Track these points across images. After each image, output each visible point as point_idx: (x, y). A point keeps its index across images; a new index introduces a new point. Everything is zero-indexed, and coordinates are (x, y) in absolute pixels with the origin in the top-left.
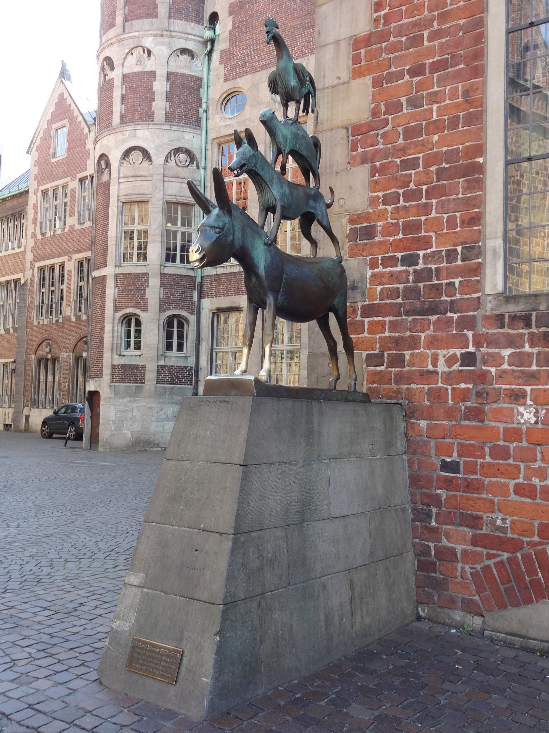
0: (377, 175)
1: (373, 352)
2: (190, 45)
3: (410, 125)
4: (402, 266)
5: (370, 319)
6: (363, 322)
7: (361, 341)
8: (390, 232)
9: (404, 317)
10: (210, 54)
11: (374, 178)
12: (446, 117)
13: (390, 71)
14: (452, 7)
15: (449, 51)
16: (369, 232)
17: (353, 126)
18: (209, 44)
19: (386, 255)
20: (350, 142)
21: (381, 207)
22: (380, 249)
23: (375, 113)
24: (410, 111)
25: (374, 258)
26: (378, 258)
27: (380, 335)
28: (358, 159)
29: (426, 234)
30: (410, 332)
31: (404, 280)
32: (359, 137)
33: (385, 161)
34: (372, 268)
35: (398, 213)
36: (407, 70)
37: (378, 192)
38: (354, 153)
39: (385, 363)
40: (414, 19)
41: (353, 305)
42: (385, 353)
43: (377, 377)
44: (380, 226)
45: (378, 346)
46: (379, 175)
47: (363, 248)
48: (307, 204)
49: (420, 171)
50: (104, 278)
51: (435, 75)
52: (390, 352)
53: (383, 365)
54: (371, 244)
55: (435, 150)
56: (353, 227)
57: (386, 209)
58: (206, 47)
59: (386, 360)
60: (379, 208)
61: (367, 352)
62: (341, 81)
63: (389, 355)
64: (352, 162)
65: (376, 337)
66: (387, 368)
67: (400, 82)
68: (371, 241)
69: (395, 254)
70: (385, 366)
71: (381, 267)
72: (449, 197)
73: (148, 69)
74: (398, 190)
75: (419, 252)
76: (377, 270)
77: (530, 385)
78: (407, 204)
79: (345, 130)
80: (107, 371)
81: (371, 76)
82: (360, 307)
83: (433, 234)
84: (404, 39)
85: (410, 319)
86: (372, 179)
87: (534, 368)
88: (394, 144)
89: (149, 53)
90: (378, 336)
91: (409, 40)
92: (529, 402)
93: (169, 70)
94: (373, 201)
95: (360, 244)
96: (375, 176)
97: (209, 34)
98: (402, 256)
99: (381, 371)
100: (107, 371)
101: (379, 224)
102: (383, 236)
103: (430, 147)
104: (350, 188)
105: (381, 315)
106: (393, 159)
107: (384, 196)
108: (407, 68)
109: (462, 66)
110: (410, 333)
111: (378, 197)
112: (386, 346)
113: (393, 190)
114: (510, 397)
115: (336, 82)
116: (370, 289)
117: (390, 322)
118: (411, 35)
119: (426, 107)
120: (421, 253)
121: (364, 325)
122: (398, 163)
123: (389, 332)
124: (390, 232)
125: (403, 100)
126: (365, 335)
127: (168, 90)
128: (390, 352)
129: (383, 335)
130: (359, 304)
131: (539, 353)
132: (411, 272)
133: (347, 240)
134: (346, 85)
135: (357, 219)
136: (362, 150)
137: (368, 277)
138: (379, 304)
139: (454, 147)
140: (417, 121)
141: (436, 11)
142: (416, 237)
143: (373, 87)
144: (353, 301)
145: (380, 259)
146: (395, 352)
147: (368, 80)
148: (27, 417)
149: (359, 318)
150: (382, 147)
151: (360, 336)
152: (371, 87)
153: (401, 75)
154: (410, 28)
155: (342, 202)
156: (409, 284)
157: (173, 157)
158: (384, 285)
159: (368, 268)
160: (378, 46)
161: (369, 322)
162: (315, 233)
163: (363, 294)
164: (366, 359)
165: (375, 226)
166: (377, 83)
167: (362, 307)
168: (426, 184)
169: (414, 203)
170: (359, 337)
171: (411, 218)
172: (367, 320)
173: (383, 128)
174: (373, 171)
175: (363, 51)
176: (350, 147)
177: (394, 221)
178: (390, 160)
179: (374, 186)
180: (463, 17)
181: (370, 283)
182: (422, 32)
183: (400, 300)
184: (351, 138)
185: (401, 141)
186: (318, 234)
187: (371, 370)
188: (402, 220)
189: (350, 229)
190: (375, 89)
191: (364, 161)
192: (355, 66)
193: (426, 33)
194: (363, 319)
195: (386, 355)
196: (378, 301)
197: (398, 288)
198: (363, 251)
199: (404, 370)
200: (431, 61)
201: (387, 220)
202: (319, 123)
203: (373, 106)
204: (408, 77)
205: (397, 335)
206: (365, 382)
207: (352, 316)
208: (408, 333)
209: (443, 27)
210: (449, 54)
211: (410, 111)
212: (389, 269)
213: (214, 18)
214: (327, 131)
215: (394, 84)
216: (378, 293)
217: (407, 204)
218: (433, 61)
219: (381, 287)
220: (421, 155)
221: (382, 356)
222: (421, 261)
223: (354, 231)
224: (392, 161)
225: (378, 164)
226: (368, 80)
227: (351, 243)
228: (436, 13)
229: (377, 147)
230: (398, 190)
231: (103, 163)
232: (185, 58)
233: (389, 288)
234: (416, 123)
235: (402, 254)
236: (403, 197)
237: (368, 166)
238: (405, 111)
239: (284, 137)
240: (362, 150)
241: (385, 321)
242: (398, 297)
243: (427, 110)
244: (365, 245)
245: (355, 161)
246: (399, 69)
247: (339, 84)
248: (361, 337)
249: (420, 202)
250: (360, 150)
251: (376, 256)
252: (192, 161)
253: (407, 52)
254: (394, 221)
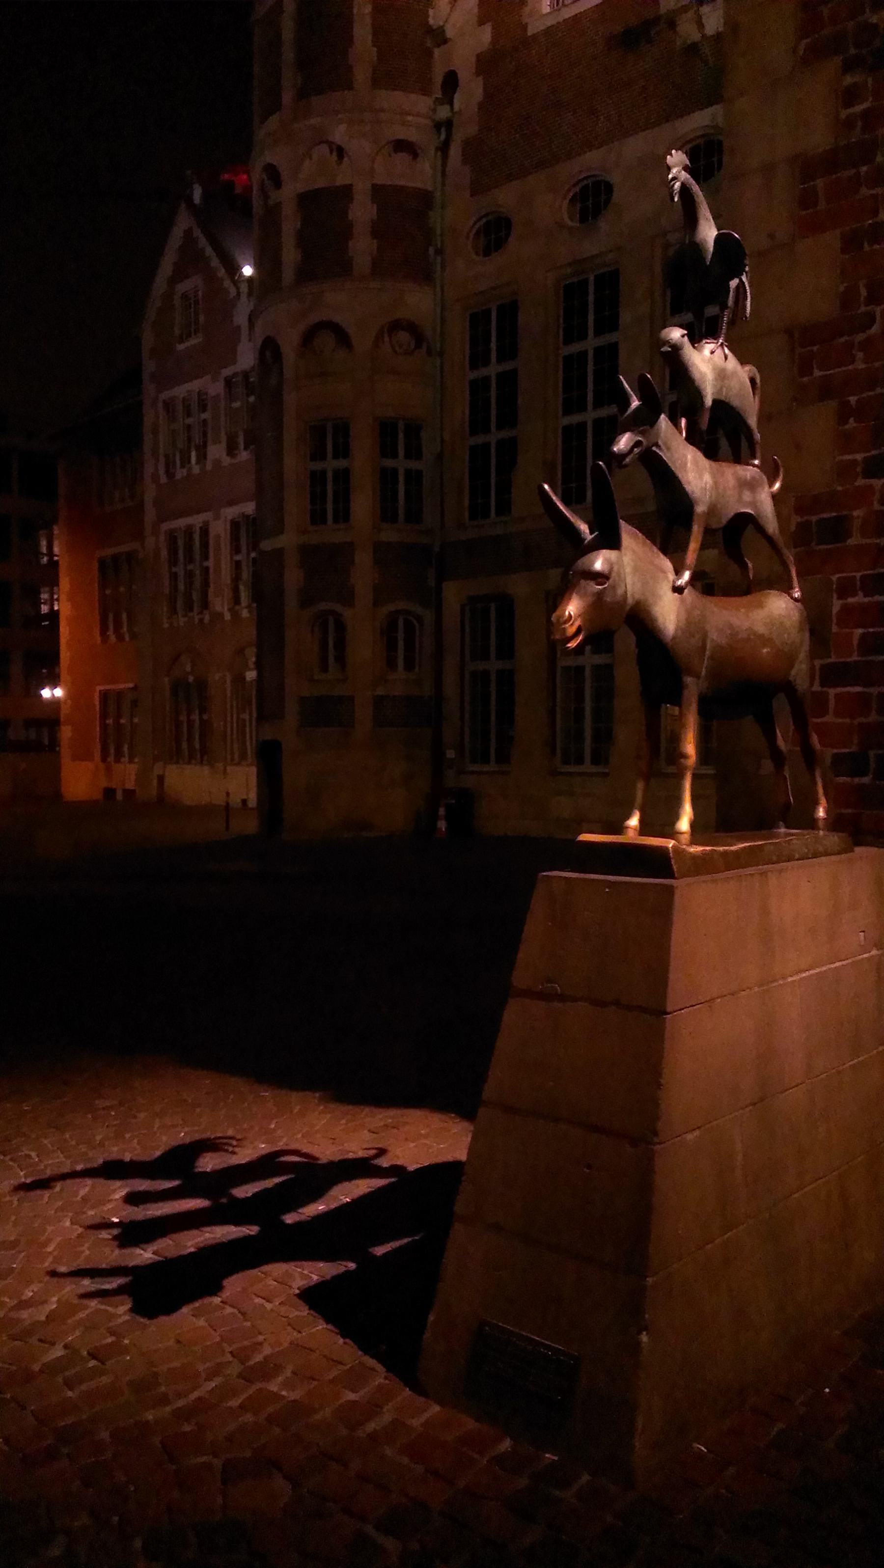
2: (412, 135)
5: (839, 690)
10: (444, 149)
16: (836, 530)
18: (443, 130)
21: (860, 482)
23: (847, 300)
38: (805, 379)
42: (872, 753)
44: (858, 517)
48: (740, 500)
50: (279, 553)
57: (871, 486)
58: (439, 138)
60: (857, 484)
71: (861, 594)
73: (340, 181)
76: (851, 600)
80: (292, 708)
89: (341, 152)
93: (375, 181)
94: (845, 471)
96: (847, 423)
97: (443, 112)
100: (292, 708)
101: (855, 513)
127: (375, 218)
136: (822, 373)
138: (855, 662)
143: (843, 251)
147: (832, 239)
148: (161, 779)
157: (386, 339)
159: (835, 596)
161: (836, 695)
166: (851, 243)
172: (832, 692)
175: (820, 183)
189: (799, 525)
194: (825, 689)
196: (855, 658)
203: (842, 288)
213: (451, 81)
216: (855, 642)
223: (804, 527)
225: (853, 399)
226: (832, 239)
229: (850, 367)
231: (268, 354)
232: (402, 158)
237: (833, 404)
239: (703, 375)
240: (822, 373)
250: (817, 373)
252: (418, 346)
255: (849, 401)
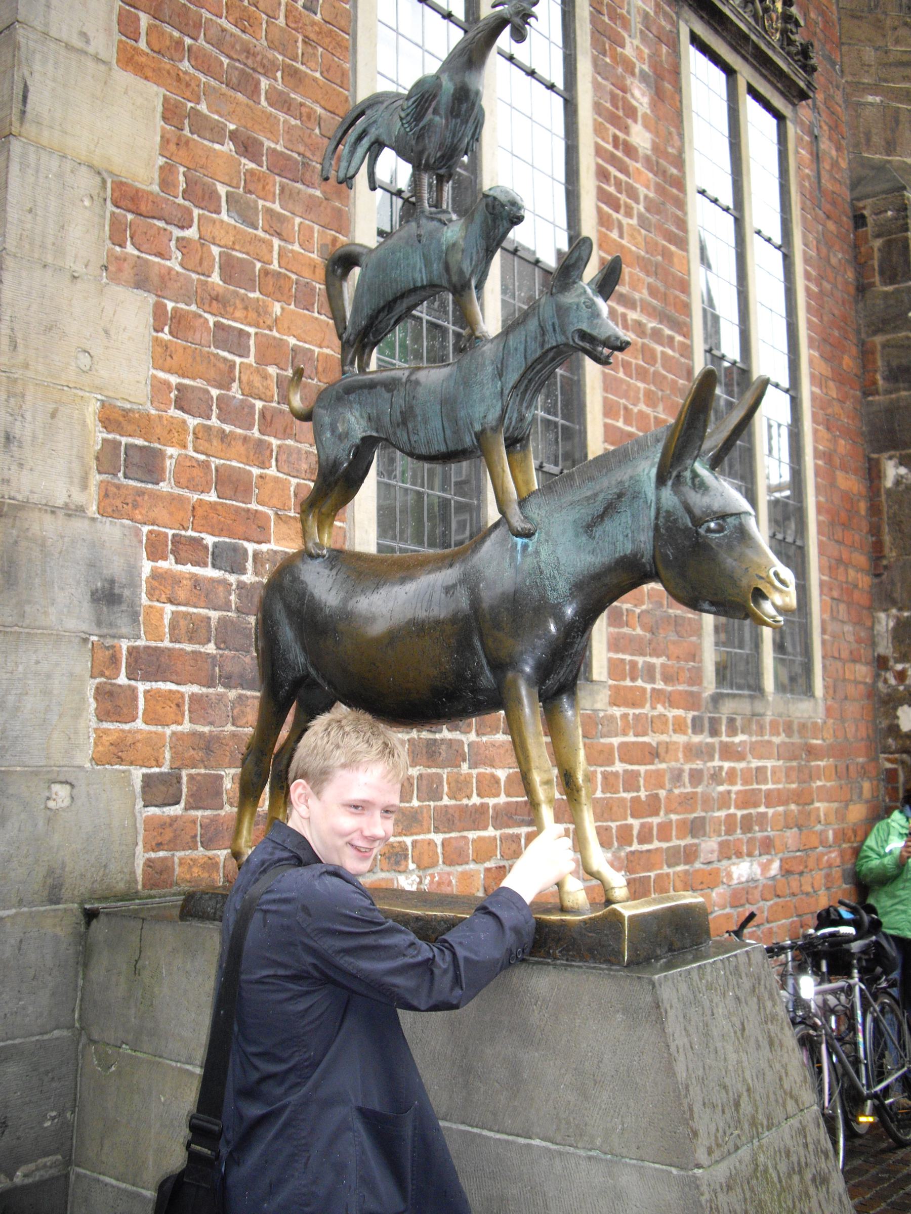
0: (166, 329)
1: (156, 770)
3: (234, 253)
4: (214, 566)
5: (148, 686)
6: (134, 690)
7: (130, 740)
8: (193, 479)
9: (220, 689)
11: (160, 335)
12: (294, 277)
13: (198, 107)
14: (303, 68)
15: (301, 149)
17: (115, 179)
19: (183, 533)
20: (108, 215)
22: (171, 514)
24: (233, 222)
25: (158, 534)
26: (166, 535)
27: (174, 727)
28: (128, 272)
29: (260, 508)
30: (233, 724)
31: (221, 601)
32: (130, 217)
33: (182, 306)
34: (152, 557)
35: (209, 441)
36: (230, 132)
37: (170, 371)
38: (118, 249)
39: (184, 797)
40: (243, 36)
41: (109, 642)
42: (184, 773)
43: (168, 835)
44: (171, 457)
45: (168, 755)
46: (171, 333)
47: (135, 500)
49: (251, 365)
51: (278, 179)
52: (193, 771)
53: (177, 803)
54: (156, 497)
55: (275, 333)
56: (110, 436)
59: (185, 790)
61: (145, 770)
62: (91, 50)
63: (191, 777)
64: (112, 268)
65: (164, 734)
66: (186, 809)
67: (217, 147)
68: (150, 486)
69: (203, 535)
70: (182, 804)
71: (171, 557)
72: (299, 445)
74: (210, 388)
75: (246, 544)
76: (162, 564)
77: (412, 834)
78: (228, 428)
79: (98, 179)
81: (162, 91)
82: (124, 652)
83: (271, 513)
84: (226, 61)
85: (232, 694)
86: (155, 334)
87: (415, 803)
88: (202, 278)
90: (168, 731)
91: (237, 73)
92: (412, 866)
95: (127, 487)
96: (162, 331)
98: (215, 545)
99: (174, 819)
101: (170, 451)
102: (178, 484)
103: (269, 322)
104: (106, 332)
105: (174, 678)
106: (201, 312)
107: (180, 388)
108: (232, 127)
109: (318, 193)
110: (234, 728)
111: (167, 384)
112: (186, 755)
113: (199, 383)
114: (389, 858)
115: (77, 42)
116: (150, 607)
117: (193, 697)
118: (237, 64)
119: (260, 233)
120: (250, 547)
121: (135, 698)
122: (211, 324)
123: (190, 722)
124: (193, 479)
125: (222, 190)
126: (139, 724)
128: (193, 771)
129: (179, 728)
130: (125, 645)
131: (421, 776)
132: (234, 587)
133: (94, 464)
134: (102, 67)
135: (121, 419)
137: (144, 577)
139: (307, 346)
140: (248, 254)
141: (280, 53)
142: (243, 509)
143: (164, 118)
144: (111, 632)
145: (170, 537)
146: (203, 771)
149: (122, 680)
150: (178, 269)
151: (126, 727)
152: (158, 115)
153: (217, 133)
154: (238, 47)
155: (85, 360)
156: (229, 614)
158: (179, 604)
159: (144, 554)
160: (176, 34)
161: (146, 692)
162: (10, 418)
163: (134, 617)
164: (143, 787)
165: (160, 454)
167: (131, 651)
168: (260, 399)
169: (239, 431)
170: (123, 731)
171: (234, 464)
172: (142, 687)
173: (182, 228)
174: (159, 317)
176: (107, 228)
177: (202, 457)
178: (193, 308)
179: (162, 355)
180: (323, 103)
181: (150, 595)
182: (256, 76)
183: (211, 648)
184: (110, 207)
185: (215, 278)
186: (18, 423)
187: (154, 815)
188: (217, 461)
189: (105, 441)
190: (168, 127)
191: (141, 282)
192: (124, 38)
193: (264, 83)
194: (133, 683)
195: (185, 779)
196: (167, 644)
197: (209, 618)
198: (135, 506)
199: (222, 813)
200: (273, 146)
201: (185, 447)
202: (29, 116)
203: (161, 161)
204: (233, 148)
205: (206, 729)
206: (140, 848)
207: (107, 673)
208: (230, 728)
209: (293, 96)
210: (299, 154)
211: (233, 222)
212: (189, 568)
214: (52, 152)
215: (206, 142)
216: (166, 622)
217: (228, 428)
218: (274, 150)
219: (174, 608)
220: (252, 330)
221: (179, 782)
222: (249, 565)
224: (200, 316)
227: (104, 476)
228: (280, 58)
229: (168, 263)
230: (210, 388)
233: (191, 614)
234: (244, 256)
235: (216, 539)
236: (218, 407)
238: (224, 216)
240: (136, 253)
241: (182, 695)
242: (209, 641)
243: (263, 241)
244: (141, 493)
245: (120, 270)
246: (216, 117)
247: (86, 53)
248: (129, 731)
249: (248, 433)
251: (164, 530)
253: (231, 93)
254: (202, 457)
255: (165, 306)
